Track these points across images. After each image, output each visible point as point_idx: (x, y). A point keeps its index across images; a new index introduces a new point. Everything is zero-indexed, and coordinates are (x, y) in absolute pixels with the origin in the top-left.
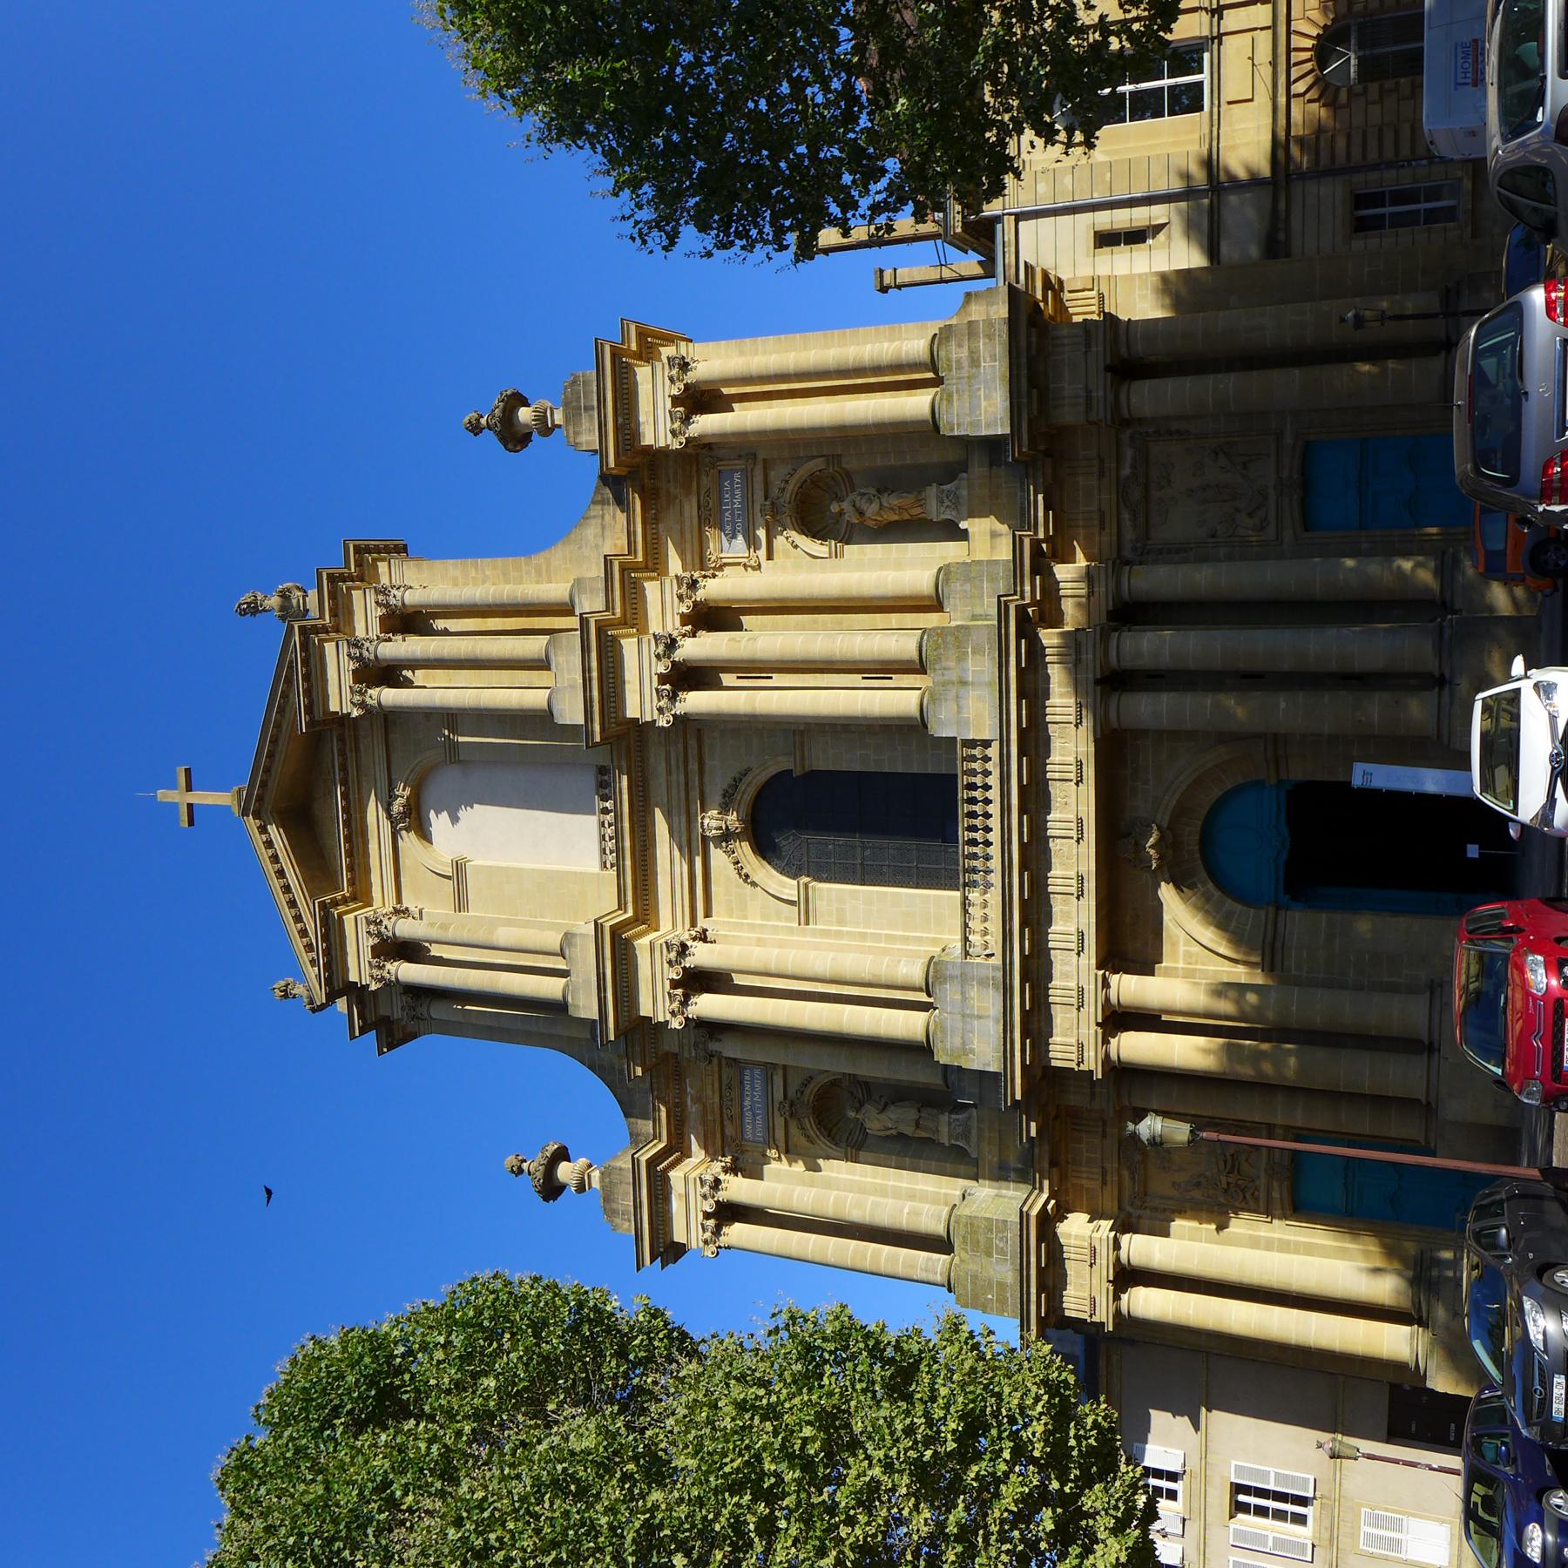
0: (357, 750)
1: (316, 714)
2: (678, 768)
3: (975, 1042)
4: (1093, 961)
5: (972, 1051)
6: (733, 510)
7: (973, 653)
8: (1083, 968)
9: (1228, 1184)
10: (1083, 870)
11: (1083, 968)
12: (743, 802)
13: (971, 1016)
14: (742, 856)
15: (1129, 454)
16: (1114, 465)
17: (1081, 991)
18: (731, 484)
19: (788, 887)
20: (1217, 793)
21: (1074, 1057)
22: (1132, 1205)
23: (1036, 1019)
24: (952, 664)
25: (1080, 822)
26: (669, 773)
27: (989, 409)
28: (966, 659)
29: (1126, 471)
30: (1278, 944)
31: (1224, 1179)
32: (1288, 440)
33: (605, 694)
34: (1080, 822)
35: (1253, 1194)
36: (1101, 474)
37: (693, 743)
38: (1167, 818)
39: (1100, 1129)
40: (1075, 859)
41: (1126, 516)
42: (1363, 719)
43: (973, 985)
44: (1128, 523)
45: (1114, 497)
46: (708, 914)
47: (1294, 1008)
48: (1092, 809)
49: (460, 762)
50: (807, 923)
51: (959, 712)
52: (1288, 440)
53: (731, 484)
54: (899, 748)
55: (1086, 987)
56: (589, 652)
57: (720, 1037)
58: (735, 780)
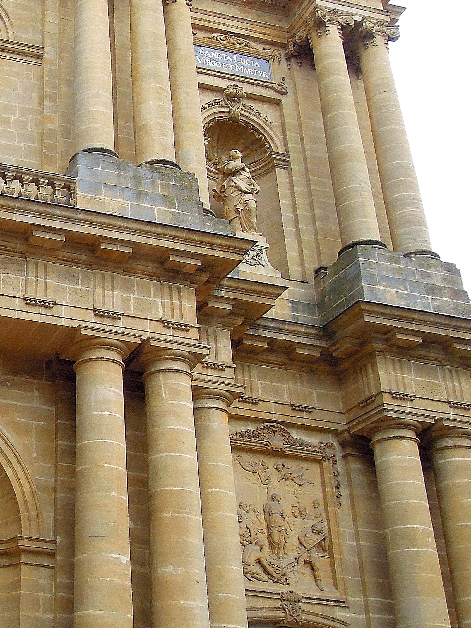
15: (313, 440)
36: (296, 408)
44: (244, 429)
45: (273, 418)
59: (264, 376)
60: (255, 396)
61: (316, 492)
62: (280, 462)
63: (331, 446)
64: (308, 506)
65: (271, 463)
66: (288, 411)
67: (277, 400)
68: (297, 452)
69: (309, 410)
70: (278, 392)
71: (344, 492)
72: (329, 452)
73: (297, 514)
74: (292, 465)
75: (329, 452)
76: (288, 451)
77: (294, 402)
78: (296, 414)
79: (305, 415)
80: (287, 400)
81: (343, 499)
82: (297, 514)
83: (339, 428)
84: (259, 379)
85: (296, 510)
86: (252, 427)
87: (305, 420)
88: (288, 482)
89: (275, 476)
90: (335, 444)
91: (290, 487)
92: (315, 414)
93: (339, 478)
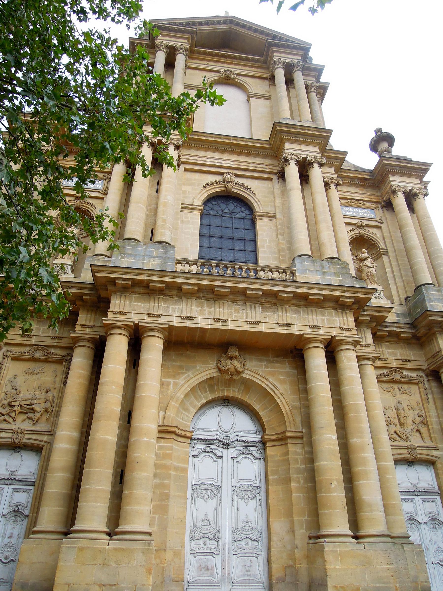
0: (252, 67)
1: (274, 47)
2: (256, 167)
3: (128, 260)
4: (175, 324)
5: (123, 258)
6: (358, 212)
7: (340, 280)
8: (171, 319)
9: (14, 406)
10: (229, 323)
11: (171, 319)
12: (239, 191)
13: (144, 259)
14: (213, 187)
15: (413, 374)
16: (409, 367)
17: (157, 316)
18: (369, 213)
19: (199, 202)
20: (257, 407)
21: (117, 309)
22: (7, 351)
23: (141, 290)
24: (332, 270)
25: (257, 323)
26: (253, 163)
27: (438, 307)
28: (336, 276)
29: (405, 373)
30: (173, 436)
31: (17, 403)
32: (434, 453)
33: (296, 135)
34: (257, 323)
35: (5, 420)
36: (404, 361)
37: (266, 175)
38: (247, 376)
39: (57, 335)
40: (234, 319)
41: (385, 371)
42: (333, 486)
43: (162, 262)
44: (382, 372)
45: (395, 366)
46: (185, 170)
47: (145, 439)
48: (264, 330)
49: (248, 100)
50: (182, 208)
51: (309, 270)
52: (434, 453)
53: (369, 213)
54: (271, 256)
55: (160, 319)
56: (317, 131)
57: (125, 165)
58: (251, 188)
59: (388, 348)
60: (385, 357)
61: (417, 398)
62: (400, 386)
63: (421, 376)
64: (414, 404)
65: (396, 386)
66: (401, 362)
67: (396, 358)
68: (407, 380)
69: (410, 361)
70: (395, 354)
71: (430, 396)
72: (421, 379)
73: (410, 409)
74: (405, 386)
75: (421, 379)
76: (403, 380)
77: (403, 358)
78: (404, 363)
79: (408, 363)
80: (399, 358)
81: (430, 400)
82: (410, 409)
83: (424, 368)
84: (386, 349)
85: (409, 407)
86: (385, 371)
87: (408, 366)
88: (404, 395)
89: (398, 392)
90: (423, 375)
91: (405, 396)
92: (413, 363)
93: (427, 391)
